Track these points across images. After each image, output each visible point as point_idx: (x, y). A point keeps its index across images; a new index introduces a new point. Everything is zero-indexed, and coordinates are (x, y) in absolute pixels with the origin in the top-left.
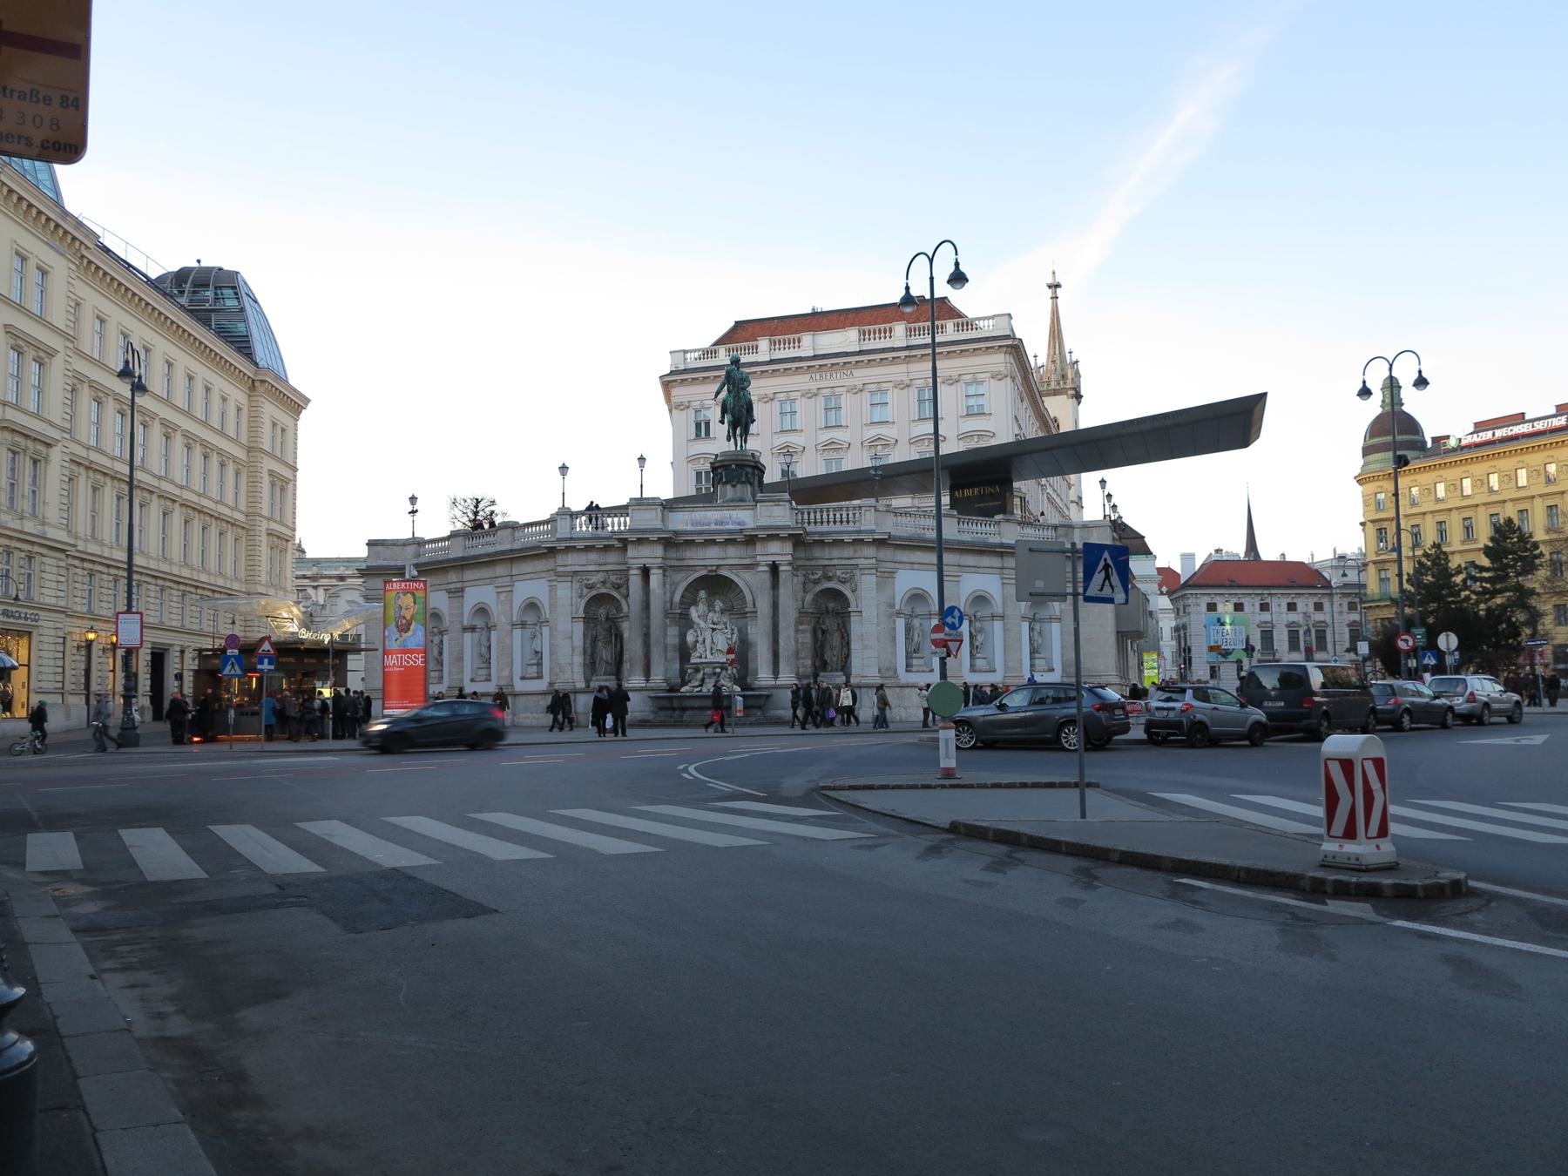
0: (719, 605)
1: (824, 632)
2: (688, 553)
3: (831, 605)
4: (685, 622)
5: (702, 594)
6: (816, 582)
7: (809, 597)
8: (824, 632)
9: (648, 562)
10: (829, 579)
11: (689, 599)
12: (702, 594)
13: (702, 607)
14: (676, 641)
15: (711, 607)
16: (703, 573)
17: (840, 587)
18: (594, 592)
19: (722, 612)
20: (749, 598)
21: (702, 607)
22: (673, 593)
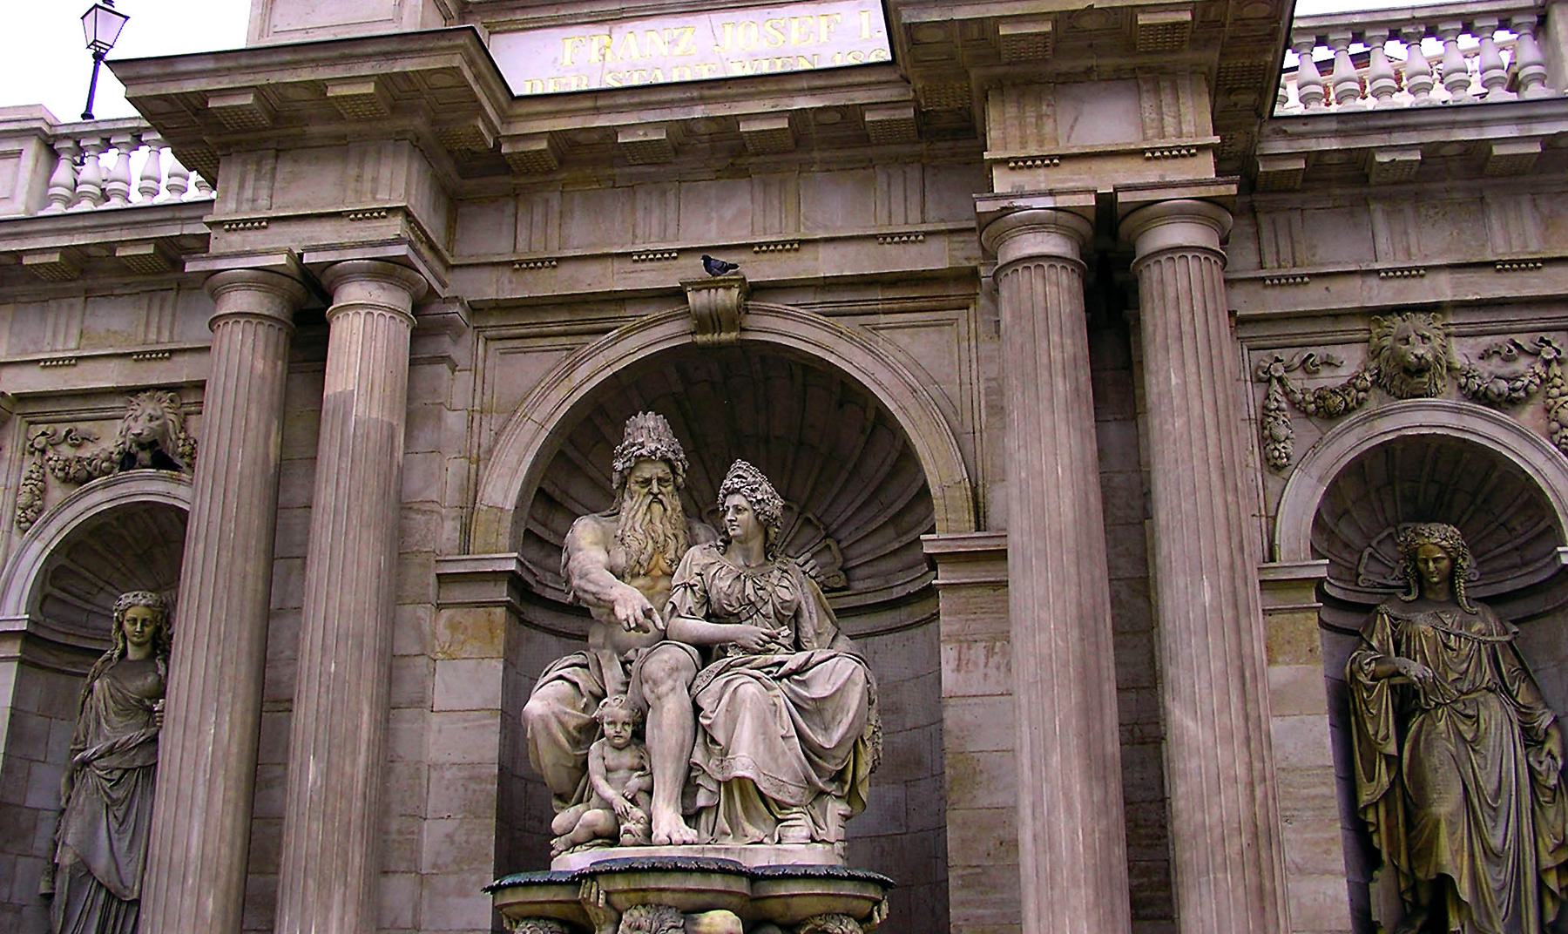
0: (747, 491)
1: (1408, 702)
2: (580, 234)
3: (1439, 537)
4: (544, 612)
5: (649, 433)
6: (1326, 411)
7: (1301, 497)
8: (1408, 702)
9: (319, 242)
10: (1407, 379)
11: (576, 469)
12: (649, 433)
13: (643, 518)
14: (487, 745)
15: (701, 507)
16: (664, 335)
17: (1484, 429)
18: (98, 500)
19: (772, 544)
20: (939, 466)
21: (643, 518)
22: (479, 460)
